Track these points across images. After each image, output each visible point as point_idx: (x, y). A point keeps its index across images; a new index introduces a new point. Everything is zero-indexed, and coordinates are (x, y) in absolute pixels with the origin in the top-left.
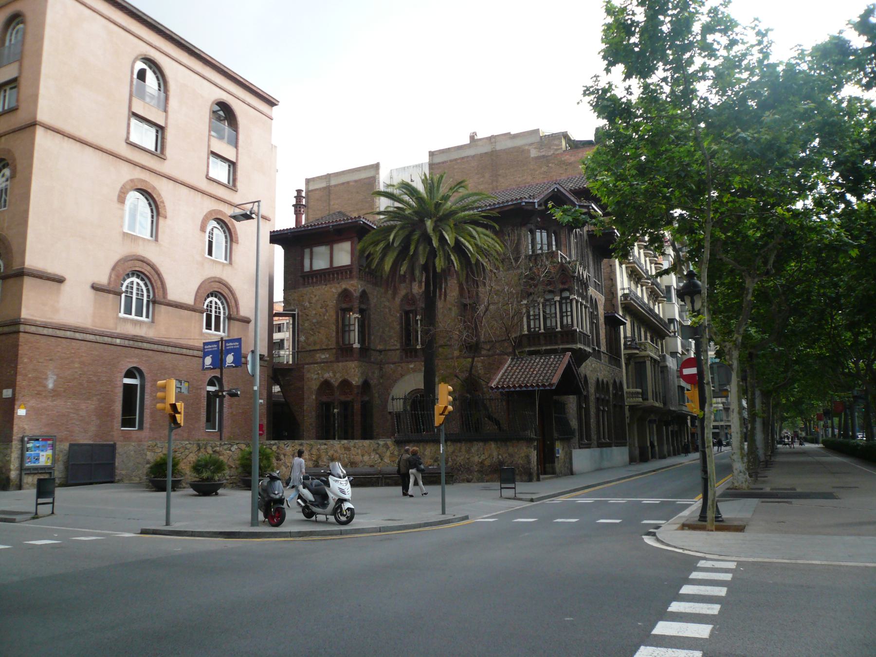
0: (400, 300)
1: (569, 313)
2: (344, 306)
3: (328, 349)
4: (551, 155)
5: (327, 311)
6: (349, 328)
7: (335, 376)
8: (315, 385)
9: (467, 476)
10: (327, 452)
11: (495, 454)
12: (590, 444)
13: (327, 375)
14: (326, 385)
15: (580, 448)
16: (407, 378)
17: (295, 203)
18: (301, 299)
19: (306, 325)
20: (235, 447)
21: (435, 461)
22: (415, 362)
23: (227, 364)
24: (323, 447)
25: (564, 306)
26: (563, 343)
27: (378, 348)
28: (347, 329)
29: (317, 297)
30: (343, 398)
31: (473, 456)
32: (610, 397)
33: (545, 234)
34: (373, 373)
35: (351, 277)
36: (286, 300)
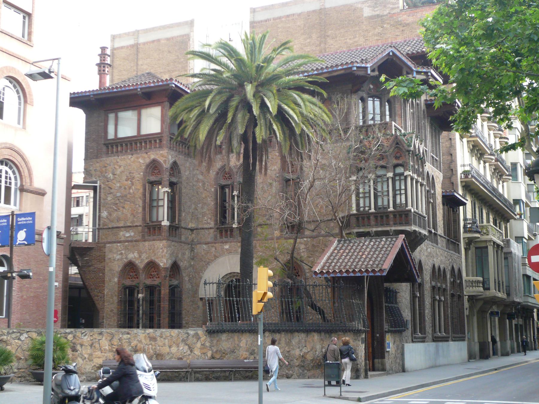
0: (215, 173)
1: (403, 192)
2: (153, 178)
3: (133, 227)
4: (387, 15)
5: (133, 184)
7: (140, 257)
8: (117, 267)
9: (287, 372)
10: (130, 343)
11: (318, 347)
12: (425, 338)
13: (132, 256)
14: (130, 266)
15: (413, 342)
16: (221, 260)
17: (98, 62)
18: (104, 169)
19: (109, 199)
20: (25, 335)
21: (251, 354)
22: (231, 242)
23: (18, 242)
24: (125, 336)
25: (397, 183)
26: (395, 224)
27: (189, 227)
28: (155, 204)
29: (122, 168)
30: (149, 282)
31: (293, 349)
32: (447, 286)
33: (377, 103)
34: (184, 254)
35: (161, 147)
36: (87, 171)
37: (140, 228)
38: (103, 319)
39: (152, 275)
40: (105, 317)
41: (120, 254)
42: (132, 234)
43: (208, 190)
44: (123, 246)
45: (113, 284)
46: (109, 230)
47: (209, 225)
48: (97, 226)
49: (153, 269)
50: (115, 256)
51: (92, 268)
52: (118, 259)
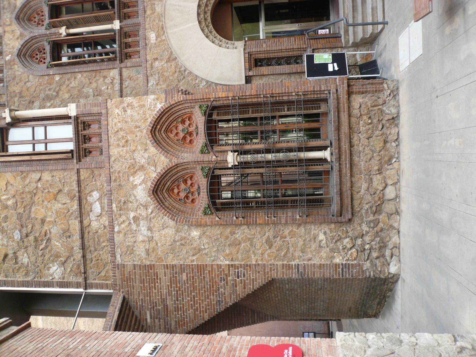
6: (39, 142)
7: (142, 168)
16: (175, 43)
19: (26, 260)
37: (84, 174)
38: (289, 267)
39: (184, 138)
40: (285, 262)
41: (138, 225)
42: (96, 195)
43: (57, 89)
44: (120, 215)
45: (205, 241)
46: (88, 256)
47: (115, 81)
48: (81, 290)
49: (172, 136)
50: (140, 238)
51: (169, 302)
52: (149, 229)
